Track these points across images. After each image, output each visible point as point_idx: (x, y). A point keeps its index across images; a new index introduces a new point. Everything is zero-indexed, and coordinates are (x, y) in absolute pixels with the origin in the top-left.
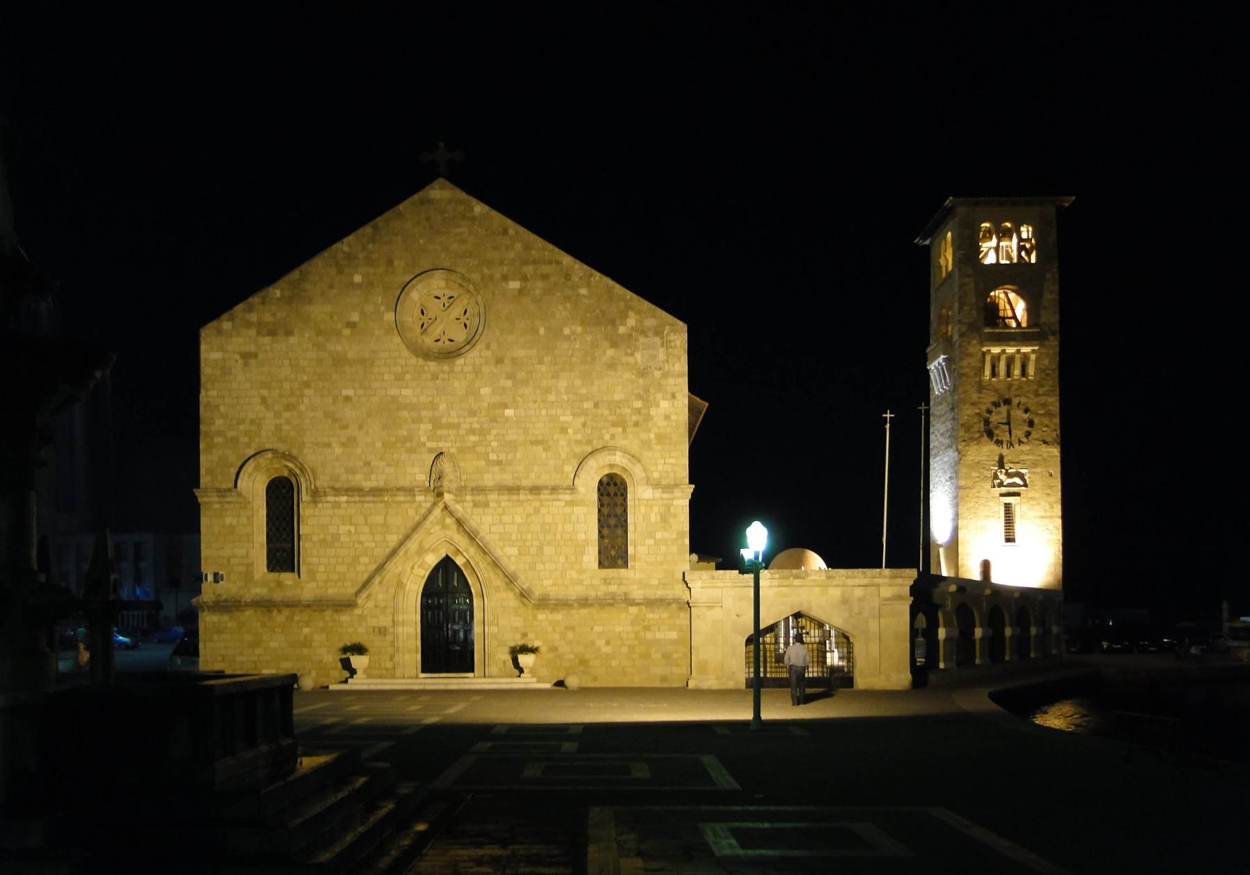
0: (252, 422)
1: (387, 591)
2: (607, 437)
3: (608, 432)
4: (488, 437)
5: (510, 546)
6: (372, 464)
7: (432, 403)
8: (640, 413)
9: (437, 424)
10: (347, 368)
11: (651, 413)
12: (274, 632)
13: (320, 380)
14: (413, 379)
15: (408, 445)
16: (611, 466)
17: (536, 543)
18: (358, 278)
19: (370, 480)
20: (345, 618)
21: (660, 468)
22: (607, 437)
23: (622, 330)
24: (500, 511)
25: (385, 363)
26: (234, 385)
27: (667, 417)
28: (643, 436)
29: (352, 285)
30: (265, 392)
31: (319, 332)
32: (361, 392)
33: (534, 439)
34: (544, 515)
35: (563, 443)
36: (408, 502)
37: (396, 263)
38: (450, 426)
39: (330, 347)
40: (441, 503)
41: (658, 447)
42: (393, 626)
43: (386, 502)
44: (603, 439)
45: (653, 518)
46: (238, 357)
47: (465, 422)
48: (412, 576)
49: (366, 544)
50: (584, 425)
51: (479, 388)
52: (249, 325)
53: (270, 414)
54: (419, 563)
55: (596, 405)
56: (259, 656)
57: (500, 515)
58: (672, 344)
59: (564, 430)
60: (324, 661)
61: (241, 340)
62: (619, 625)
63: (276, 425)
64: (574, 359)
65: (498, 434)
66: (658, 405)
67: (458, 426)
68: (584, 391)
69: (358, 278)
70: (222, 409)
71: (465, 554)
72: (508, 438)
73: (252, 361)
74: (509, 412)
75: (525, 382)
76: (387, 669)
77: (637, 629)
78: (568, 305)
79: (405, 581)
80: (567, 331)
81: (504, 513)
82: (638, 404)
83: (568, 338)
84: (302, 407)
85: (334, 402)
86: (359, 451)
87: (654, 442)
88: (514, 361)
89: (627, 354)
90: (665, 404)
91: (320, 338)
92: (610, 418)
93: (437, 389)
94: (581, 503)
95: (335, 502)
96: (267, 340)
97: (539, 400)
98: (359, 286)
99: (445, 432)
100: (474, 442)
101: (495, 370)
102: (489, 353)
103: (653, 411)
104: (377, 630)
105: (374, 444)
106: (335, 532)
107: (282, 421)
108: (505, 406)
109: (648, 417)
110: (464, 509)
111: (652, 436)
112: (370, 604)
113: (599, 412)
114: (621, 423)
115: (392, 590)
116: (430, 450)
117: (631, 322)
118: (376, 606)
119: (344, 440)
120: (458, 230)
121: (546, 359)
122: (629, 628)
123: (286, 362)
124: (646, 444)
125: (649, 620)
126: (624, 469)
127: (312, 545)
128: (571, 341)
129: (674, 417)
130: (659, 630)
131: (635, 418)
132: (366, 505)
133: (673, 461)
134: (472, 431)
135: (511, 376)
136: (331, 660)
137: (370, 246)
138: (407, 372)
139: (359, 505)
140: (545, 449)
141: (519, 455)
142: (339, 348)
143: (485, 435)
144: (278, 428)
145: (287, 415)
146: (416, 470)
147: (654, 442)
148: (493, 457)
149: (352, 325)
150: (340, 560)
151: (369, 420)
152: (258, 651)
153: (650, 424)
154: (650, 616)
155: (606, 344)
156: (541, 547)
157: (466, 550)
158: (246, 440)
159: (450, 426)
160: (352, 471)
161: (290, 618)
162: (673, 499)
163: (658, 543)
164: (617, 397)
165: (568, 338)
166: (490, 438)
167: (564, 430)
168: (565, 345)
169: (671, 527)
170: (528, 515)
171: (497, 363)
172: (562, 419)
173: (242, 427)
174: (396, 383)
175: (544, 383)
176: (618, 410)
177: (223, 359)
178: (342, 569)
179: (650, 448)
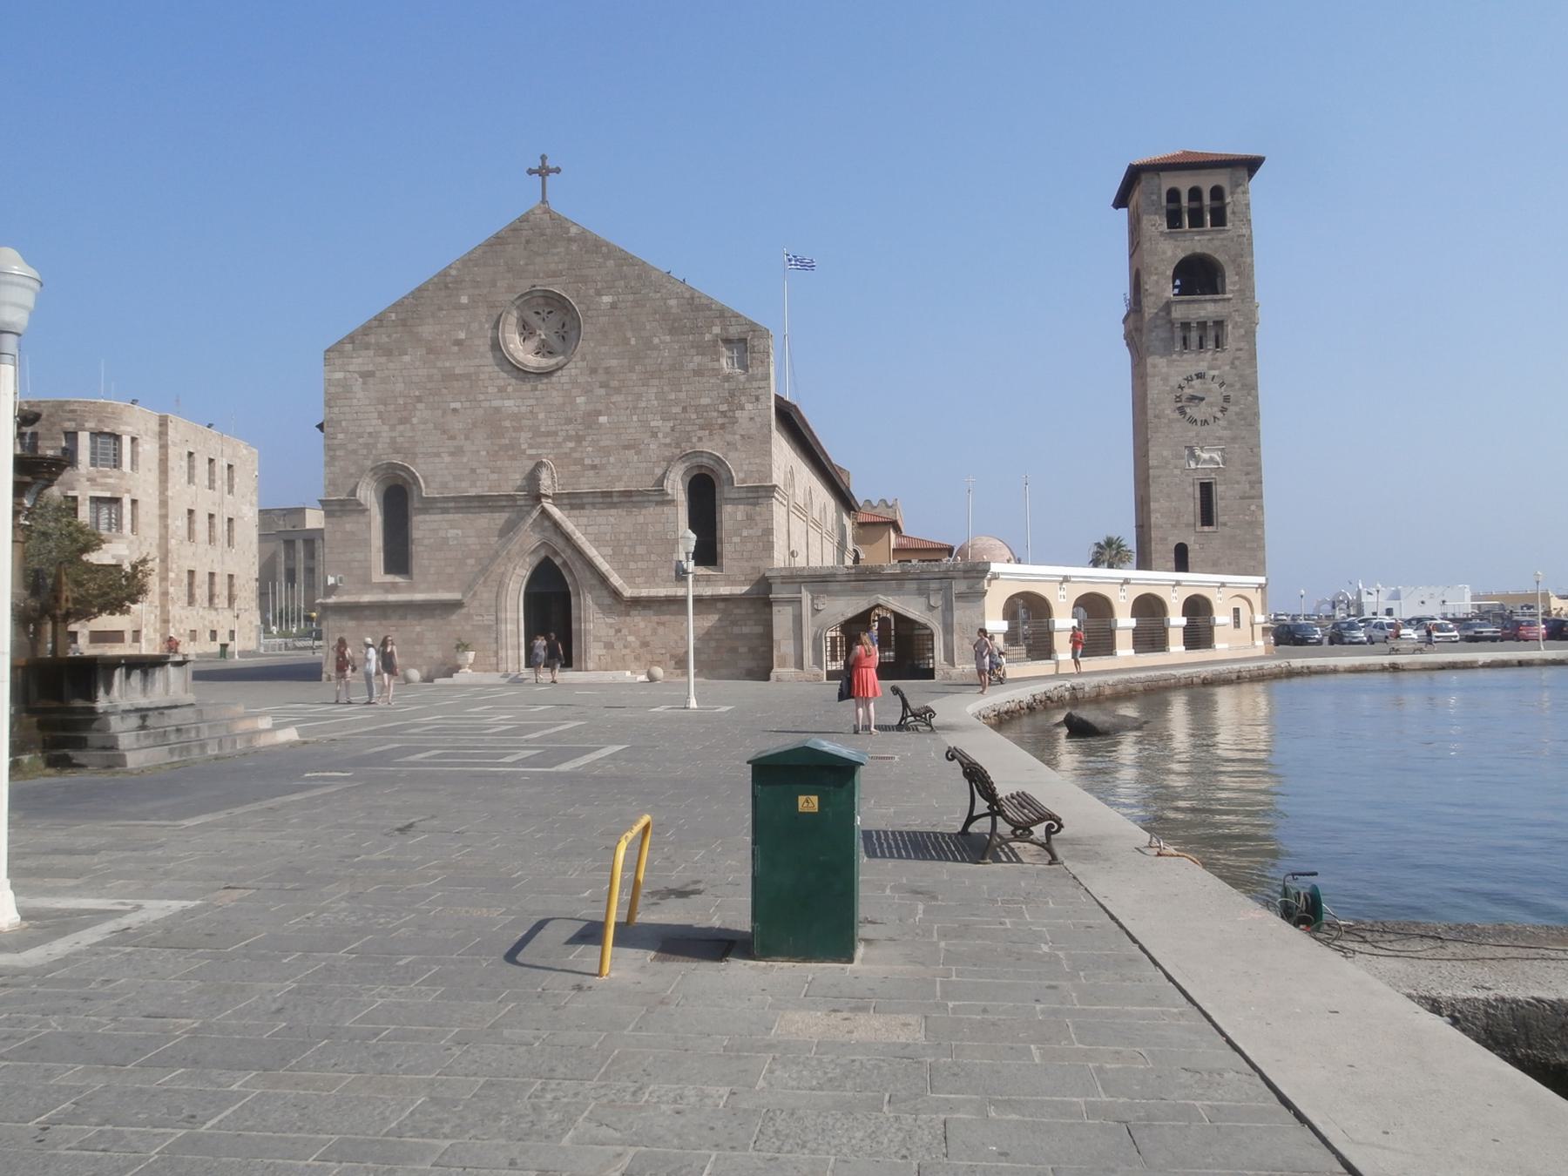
0: (370, 433)
2: (695, 440)
3: (695, 436)
4: (584, 443)
5: (605, 546)
6: (478, 471)
7: (531, 412)
8: (725, 416)
9: (536, 432)
10: (455, 382)
11: (737, 415)
13: (430, 394)
14: (515, 390)
15: (511, 453)
19: (476, 487)
21: (745, 467)
22: (695, 440)
26: (355, 401)
27: (751, 419)
28: (729, 437)
29: (459, 307)
30: (381, 408)
31: (430, 351)
33: (626, 443)
34: (636, 515)
36: (511, 506)
37: (498, 285)
38: (548, 434)
39: (439, 364)
40: (539, 507)
43: (490, 507)
44: (691, 442)
45: (739, 518)
46: (356, 375)
47: (562, 430)
48: (514, 575)
49: (473, 547)
50: (673, 429)
51: (575, 397)
52: (367, 347)
53: (386, 428)
54: (520, 564)
55: (684, 409)
59: (654, 435)
61: (360, 360)
63: (391, 437)
64: (662, 367)
65: (593, 440)
67: (555, 434)
69: (464, 300)
70: (344, 424)
71: (563, 555)
72: (602, 444)
73: (371, 380)
74: (603, 419)
75: (618, 390)
76: (490, 665)
78: (657, 316)
79: (507, 581)
80: (656, 341)
82: (724, 408)
83: (656, 348)
84: (415, 420)
85: (444, 412)
86: (465, 460)
88: (607, 370)
89: (713, 360)
90: (749, 406)
91: (432, 356)
92: (697, 422)
93: (537, 399)
96: (383, 360)
97: (631, 406)
98: (465, 307)
99: (543, 440)
100: (571, 448)
101: (590, 380)
103: (738, 414)
105: (478, 451)
106: (444, 536)
108: (599, 413)
109: (734, 421)
111: (737, 437)
112: (476, 603)
113: (687, 415)
114: (708, 426)
115: (495, 589)
116: (531, 457)
118: (481, 605)
120: (555, 251)
121: (637, 367)
123: (400, 379)
126: (712, 470)
128: (660, 350)
130: (746, 625)
131: (720, 421)
133: (758, 461)
134: (568, 438)
135: (604, 385)
136: (441, 656)
137: (476, 269)
138: (509, 385)
140: (638, 453)
141: (612, 459)
143: (581, 442)
144: (393, 440)
145: (401, 428)
148: (588, 462)
149: (458, 343)
154: (737, 611)
155: (693, 351)
156: (633, 547)
157: (564, 551)
158: (365, 452)
159: (548, 434)
162: (758, 498)
163: (744, 540)
164: (705, 401)
165: (656, 348)
167: (654, 435)
168: (655, 354)
169: (756, 525)
171: (591, 374)
172: (652, 424)
173: (361, 441)
174: (500, 394)
176: (705, 414)
177: (345, 378)
178: (450, 570)
179: (736, 449)
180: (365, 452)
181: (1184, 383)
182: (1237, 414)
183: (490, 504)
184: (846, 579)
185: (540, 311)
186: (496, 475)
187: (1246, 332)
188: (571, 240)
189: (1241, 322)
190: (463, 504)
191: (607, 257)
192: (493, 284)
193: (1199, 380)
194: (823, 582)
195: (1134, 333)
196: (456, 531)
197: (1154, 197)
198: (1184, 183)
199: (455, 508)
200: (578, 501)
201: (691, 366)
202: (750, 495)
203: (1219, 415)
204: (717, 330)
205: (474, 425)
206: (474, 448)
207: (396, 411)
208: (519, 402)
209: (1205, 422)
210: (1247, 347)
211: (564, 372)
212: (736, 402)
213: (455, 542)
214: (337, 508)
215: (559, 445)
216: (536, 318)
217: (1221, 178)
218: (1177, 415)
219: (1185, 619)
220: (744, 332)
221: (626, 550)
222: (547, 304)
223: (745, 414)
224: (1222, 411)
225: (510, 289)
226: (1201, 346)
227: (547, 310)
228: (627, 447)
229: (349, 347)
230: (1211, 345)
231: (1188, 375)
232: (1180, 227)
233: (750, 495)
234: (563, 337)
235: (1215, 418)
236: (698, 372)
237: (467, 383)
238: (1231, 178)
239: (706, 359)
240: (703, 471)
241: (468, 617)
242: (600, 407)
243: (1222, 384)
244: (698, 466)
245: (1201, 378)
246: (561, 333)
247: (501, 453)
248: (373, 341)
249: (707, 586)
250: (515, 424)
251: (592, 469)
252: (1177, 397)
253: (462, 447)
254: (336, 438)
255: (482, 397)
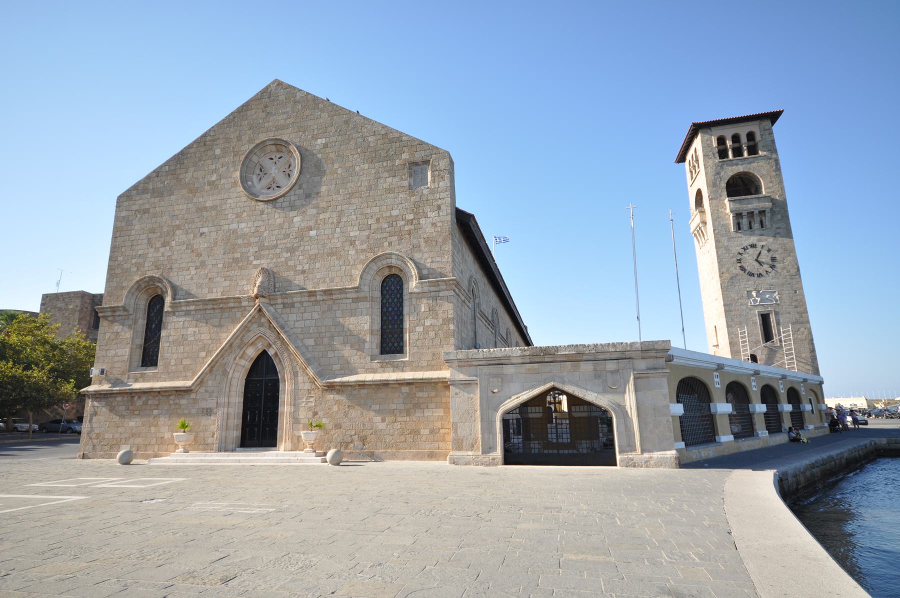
0: (140, 255)
1: (215, 379)
2: (386, 244)
12: (134, 415)
13: (186, 222)
16: (390, 267)
17: (328, 334)
18: (218, 152)
20: (183, 402)
22: (386, 244)
23: (397, 162)
24: (302, 309)
25: (230, 207)
26: (133, 232)
29: (216, 158)
32: (213, 229)
34: (335, 310)
35: (352, 252)
36: (237, 307)
38: (268, 248)
39: (195, 200)
41: (426, 250)
42: (217, 408)
49: (205, 342)
54: (240, 355)
55: (378, 221)
56: (121, 433)
57: (302, 313)
58: (438, 168)
59: (352, 243)
60: (165, 438)
61: (141, 202)
62: (393, 403)
66: (426, 217)
67: (276, 246)
68: (369, 211)
72: (312, 252)
74: (313, 233)
77: (408, 406)
79: (229, 370)
80: (357, 168)
81: (305, 312)
82: (411, 217)
84: (173, 243)
87: (423, 244)
89: (402, 179)
91: (190, 195)
94: (364, 299)
95: (187, 310)
96: (157, 200)
99: (267, 252)
100: (291, 260)
102: (302, 191)
103: (422, 221)
104: (205, 411)
107: (160, 255)
109: (418, 227)
110: (275, 309)
111: (422, 240)
113: (379, 225)
116: (256, 267)
117: (405, 156)
118: (206, 391)
119: (198, 264)
122: (402, 407)
124: (416, 247)
125: (419, 398)
127: (168, 344)
129: (439, 224)
130: (427, 408)
131: (407, 228)
132: (208, 312)
133: (438, 259)
138: (244, 211)
139: (203, 312)
140: (339, 259)
141: (318, 265)
142: (201, 200)
145: (162, 250)
146: (244, 282)
147: (423, 244)
148: (299, 268)
149: (211, 183)
150: (186, 355)
151: (216, 248)
152: (120, 430)
153: (420, 232)
155: (386, 175)
159: (268, 248)
160: (200, 286)
161: (145, 403)
162: (439, 291)
164: (395, 213)
166: (297, 253)
167: (352, 243)
168: (356, 178)
170: (323, 312)
172: (352, 234)
173: (134, 261)
175: (339, 208)
178: (185, 362)
179: (420, 251)
180: (134, 269)
181: (742, 251)
182: (784, 268)
183: (221, 306)
184: (520, 361)
185: (273, 157)
186: (228, 282)
187: (782, 217)
188: (295, 102)
189: (778, 211)
190: (201, 307)
191: (322, 111)
192: (239, 138)
193: (752, 249)
194: (498, 364)
195: (701, 225)
196: (194, 329)
197: (709, 142)
198: (728, 132)
199: (196, 310)
200: (289, 301)
201: (385, 186)
202: (432, 289)
203: (770, 270)
204: (405, 156)
205: (216, 243)
206: (214, 262)
207: (161, 237)
208: (250, 224)
209: (760, 275)
210: (784, 226)
211: (287, 199)
212: (421, 211)
213: (192, 338)
214: (110, 314)
215: (278, 256)
216: (271, 161)
217: (754, 127)
218: (739, 271)
219: (730, 405)
220: (428, 156)
221: (326, 340)
222: (278, 151)
223: (429, 220)
224: (771, 267)
225: (250, 141)
226: (751, 228)
227: (278, 156)
228: (330, 255)
229: (134, 192)
230: (756, 225)
231: (744, 245)
232: (728, 157)
233: (432, 289)
234: (289, 175)
235: (767, 271)
236: (390, 190)
237: (214, 213)
238: (759, 127)
239: (396, 179)
240: (394, 271)
241: (195, 401)
242: (312, 223)
243: (769, 250)
244: (389, 267)
245: (753, 247)
246: (288, 171)
247: (234, 265)
248: (151, 187)
249: (394, 371)
250: (246, 241)
251: (302, 274)
252: (739, 260)
253: (205, 261)
254: (117, 260)
255: (223, 222)
